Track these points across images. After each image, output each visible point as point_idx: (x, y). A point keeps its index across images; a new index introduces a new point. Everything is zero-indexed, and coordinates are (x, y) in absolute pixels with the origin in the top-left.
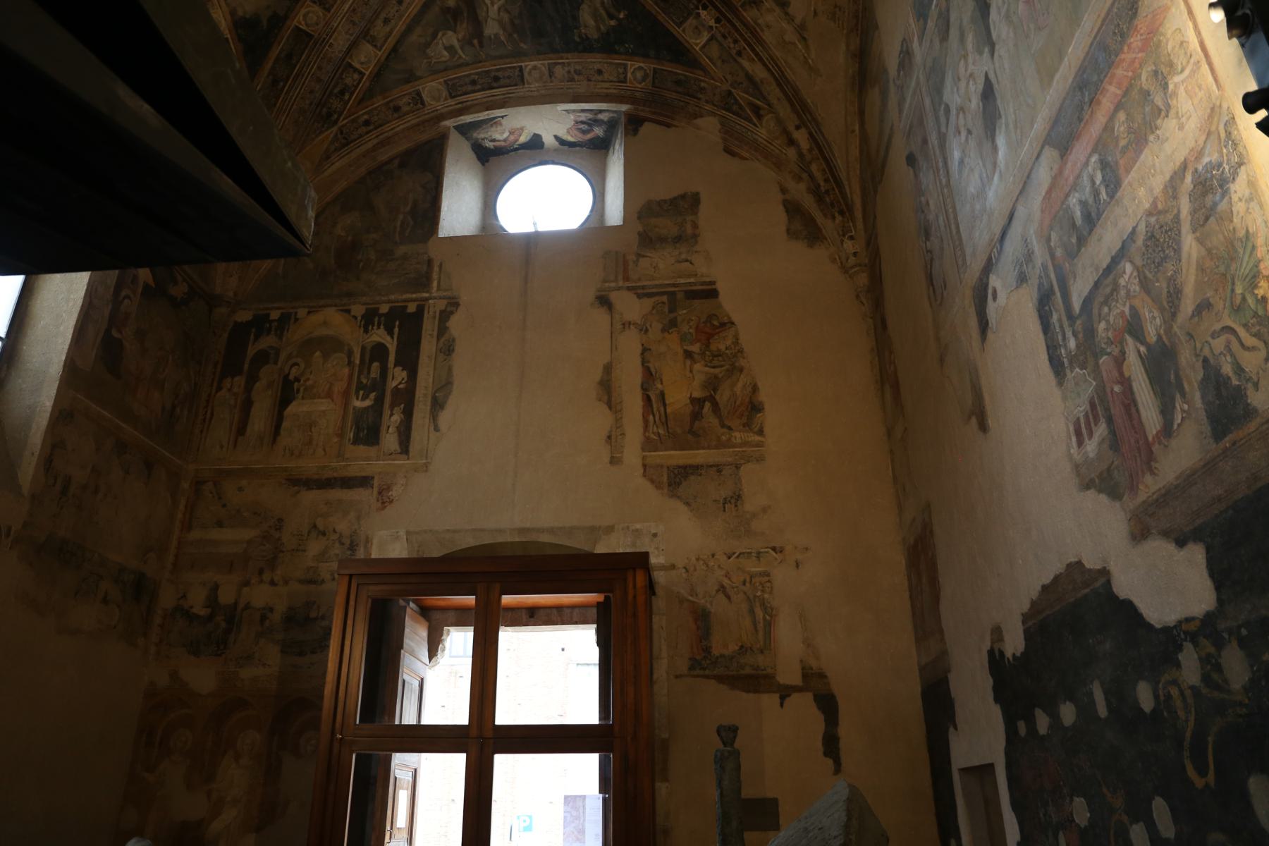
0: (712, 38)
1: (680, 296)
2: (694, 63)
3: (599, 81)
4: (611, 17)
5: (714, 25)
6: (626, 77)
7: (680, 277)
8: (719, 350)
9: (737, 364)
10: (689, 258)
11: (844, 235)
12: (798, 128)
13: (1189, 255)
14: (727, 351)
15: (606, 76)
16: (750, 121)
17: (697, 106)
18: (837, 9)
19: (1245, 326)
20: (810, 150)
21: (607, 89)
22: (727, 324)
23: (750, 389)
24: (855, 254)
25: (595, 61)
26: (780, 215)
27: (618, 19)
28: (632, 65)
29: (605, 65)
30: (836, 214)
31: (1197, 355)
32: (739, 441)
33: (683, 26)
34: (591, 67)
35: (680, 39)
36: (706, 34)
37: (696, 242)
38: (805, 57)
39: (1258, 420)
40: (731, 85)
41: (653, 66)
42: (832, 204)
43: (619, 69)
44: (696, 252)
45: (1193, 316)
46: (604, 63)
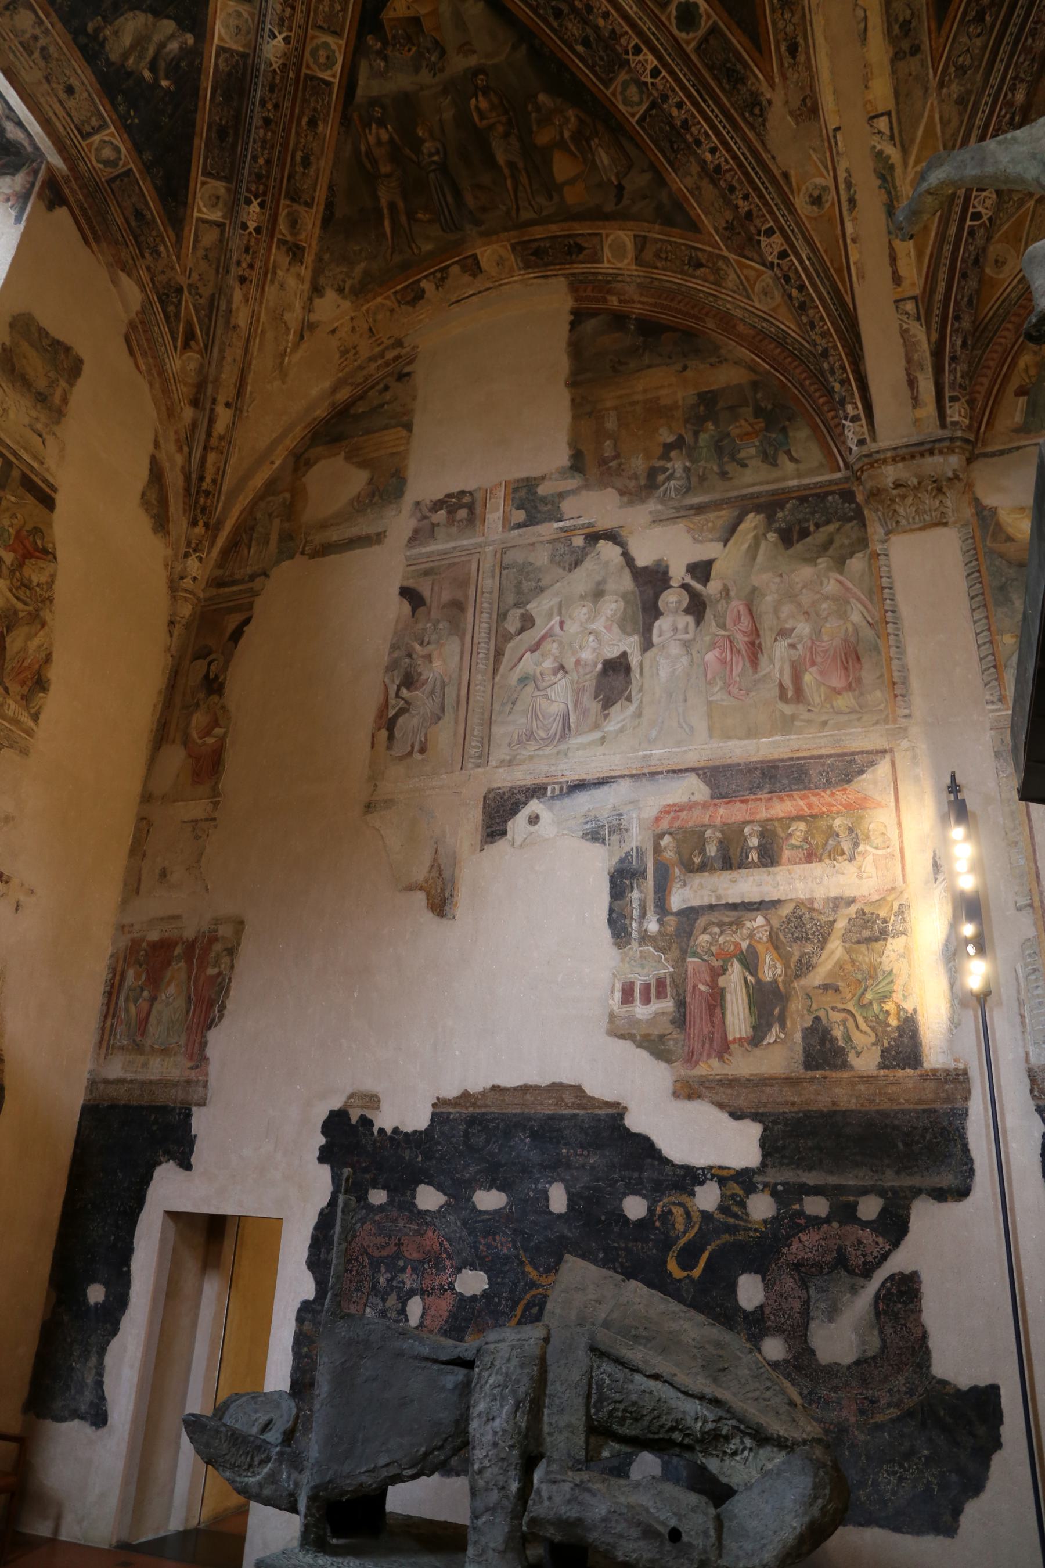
0: (220, 225)
1: (15, 474)
2: (176, 220)
3: (56, 96)
4: (153, 67)
5: (251, 228)
6: (89, 135)
7: (25, 449)
8: (30, 581)
9: (42, 613)
10: (44, 435)
11: (195, 551)
12: (228, 405)
13: (833, 952)
14: (38, 589)
15: (71, 104)
16: (174, 339)
17: (133, 258)
18: (353, 351)
19: (865, 1018)
20: (221, 438)
21: (56, 114)
22: (48, 554)
23: (43, 655)
24: (195, 579)
25: (81, 76)
26: (144, 473)
27: (156, 79)
28: (112, 135)
29: (86, 95)
30: (201, 523)
31: (809, 1011)
32: (10, 713)
33: (209, 180)
34: (67, 72)
35: (192, 184)
36: (220, 214)
37: (58, 422)
38: (285, 351)
39: (852, 1073)
40: (190, 286)
41: (132, 165)
42: (203, 510)
43: (94, 119)
44: (54, 434)
45: (819, 987)
46: (87, 91)
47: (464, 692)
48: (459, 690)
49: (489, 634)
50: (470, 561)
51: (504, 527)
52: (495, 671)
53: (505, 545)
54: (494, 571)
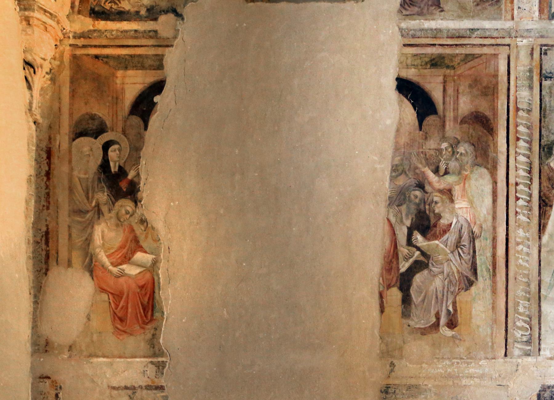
47: (501, 251)
48: (494, 247)
49: (530, 172)
50: (496, 56)
51: (541, 11)
52: (542, 228)
53: (544, 41)
54: (531, 78)
